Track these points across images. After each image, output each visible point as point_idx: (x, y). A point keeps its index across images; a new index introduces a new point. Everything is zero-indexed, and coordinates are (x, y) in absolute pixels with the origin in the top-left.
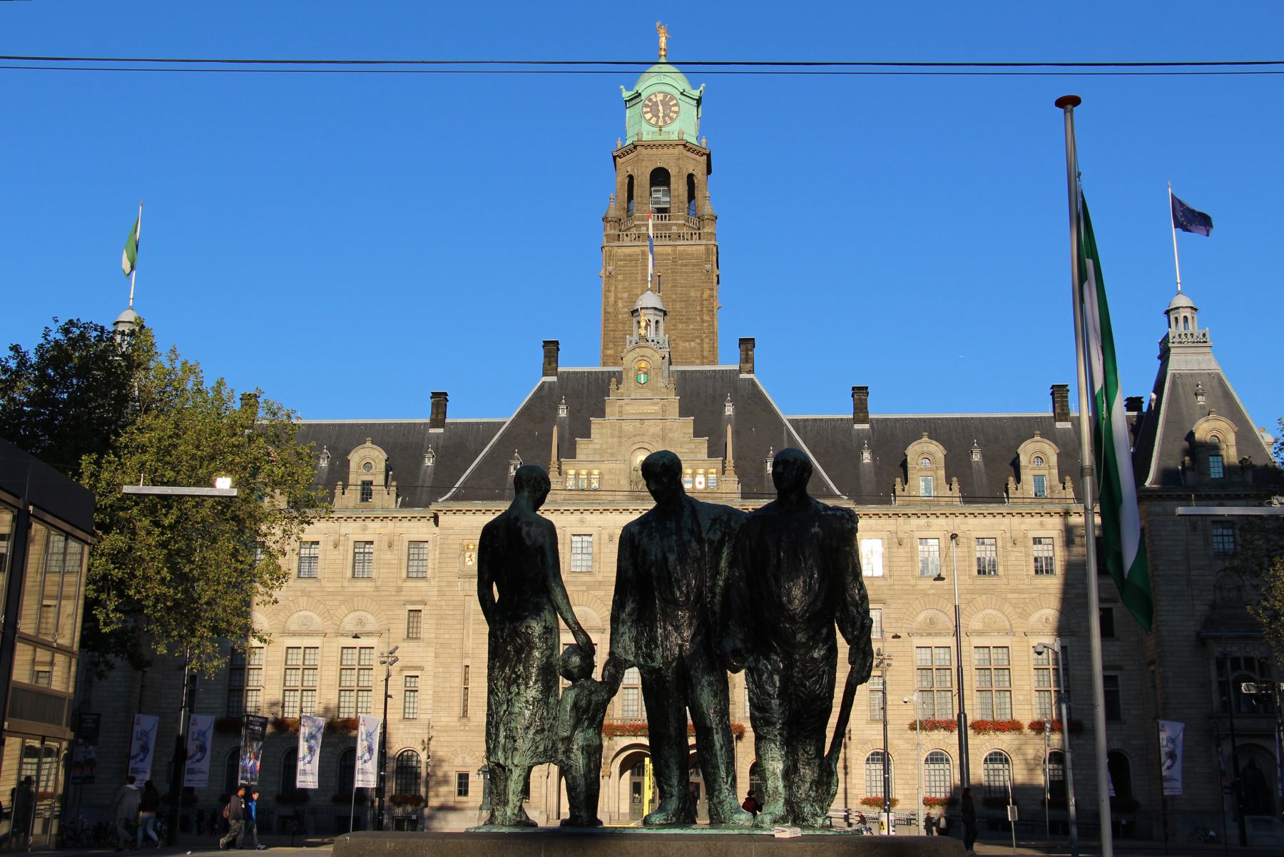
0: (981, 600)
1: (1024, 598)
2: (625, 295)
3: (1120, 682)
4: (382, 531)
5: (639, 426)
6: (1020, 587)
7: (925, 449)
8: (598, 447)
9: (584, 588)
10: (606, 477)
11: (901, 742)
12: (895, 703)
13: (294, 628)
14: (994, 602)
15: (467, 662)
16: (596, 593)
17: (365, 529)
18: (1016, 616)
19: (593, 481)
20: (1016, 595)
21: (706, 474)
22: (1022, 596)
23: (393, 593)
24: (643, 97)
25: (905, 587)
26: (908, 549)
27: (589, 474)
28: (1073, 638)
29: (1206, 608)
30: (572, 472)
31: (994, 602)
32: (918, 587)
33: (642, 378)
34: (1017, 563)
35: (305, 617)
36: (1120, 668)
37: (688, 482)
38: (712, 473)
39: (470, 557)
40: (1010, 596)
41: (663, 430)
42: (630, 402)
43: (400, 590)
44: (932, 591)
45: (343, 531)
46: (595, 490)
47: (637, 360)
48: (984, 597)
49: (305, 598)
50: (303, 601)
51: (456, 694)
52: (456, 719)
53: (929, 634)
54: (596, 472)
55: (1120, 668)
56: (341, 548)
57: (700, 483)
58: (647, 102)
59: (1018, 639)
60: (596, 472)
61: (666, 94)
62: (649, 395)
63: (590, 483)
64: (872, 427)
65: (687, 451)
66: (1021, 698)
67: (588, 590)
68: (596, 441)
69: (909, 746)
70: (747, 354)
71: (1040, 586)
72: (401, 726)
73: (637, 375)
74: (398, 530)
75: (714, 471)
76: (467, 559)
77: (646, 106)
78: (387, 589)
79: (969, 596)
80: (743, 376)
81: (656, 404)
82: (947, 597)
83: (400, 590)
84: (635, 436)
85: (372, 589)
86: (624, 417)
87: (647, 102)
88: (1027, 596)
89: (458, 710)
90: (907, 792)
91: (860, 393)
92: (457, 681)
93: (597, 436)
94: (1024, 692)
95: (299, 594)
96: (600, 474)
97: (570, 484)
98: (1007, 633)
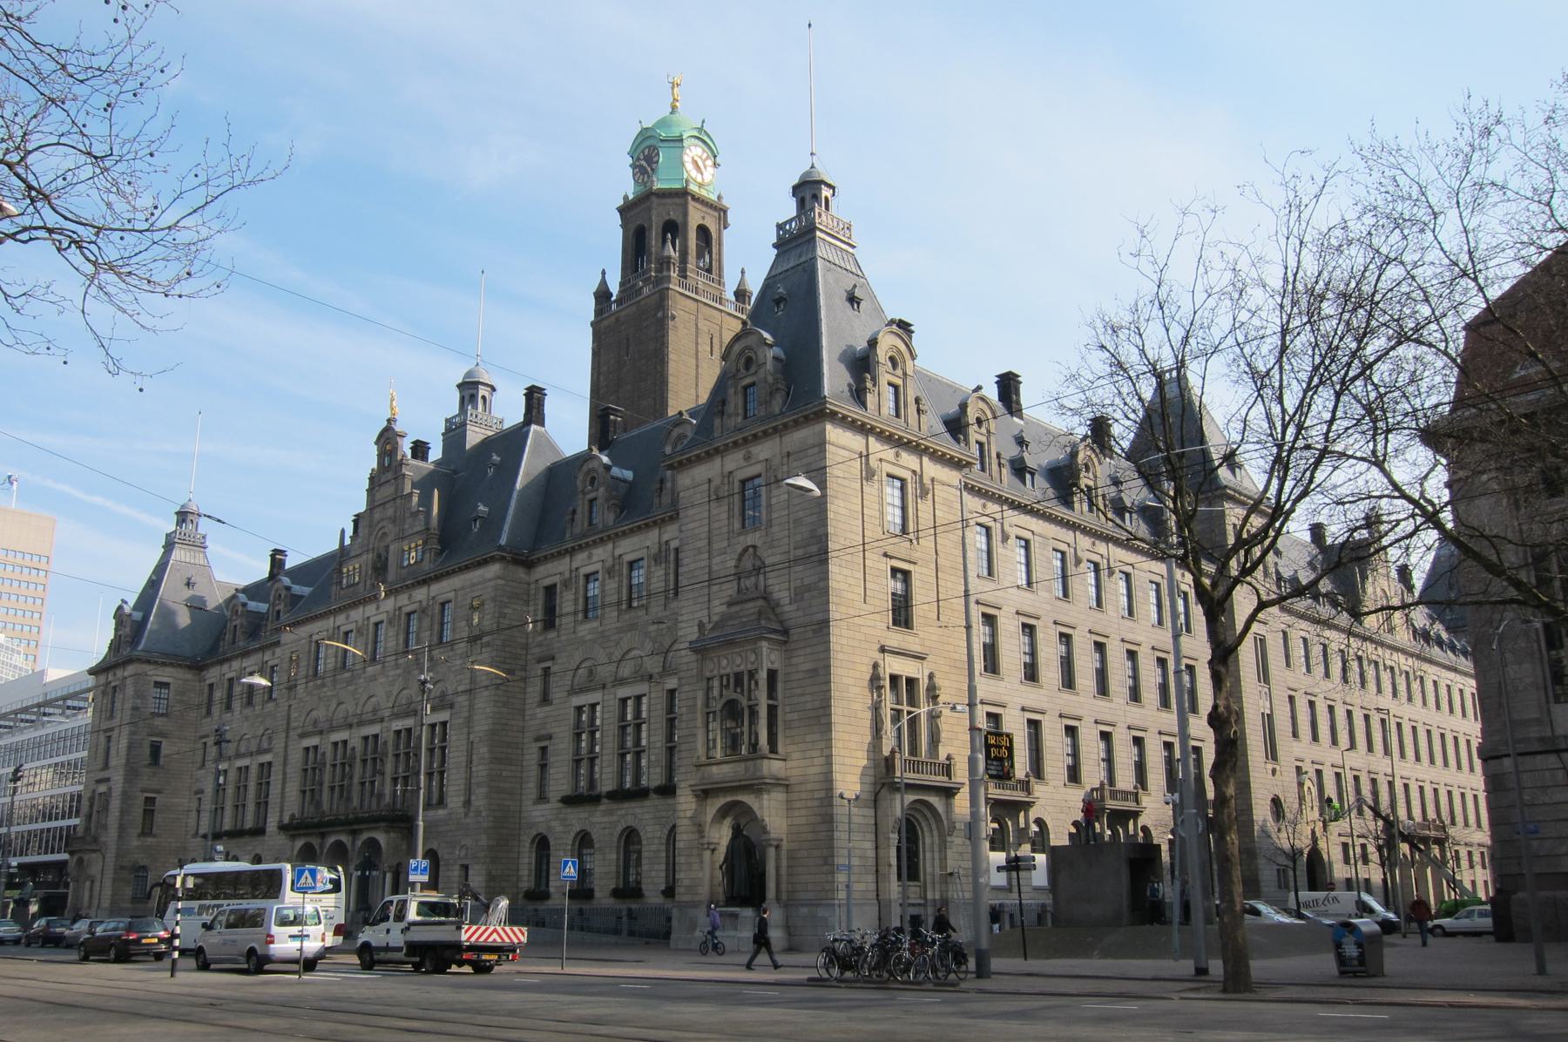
20: (655, 627)
44: (589, 637)
79: (617, 637)
94: (656, 751)
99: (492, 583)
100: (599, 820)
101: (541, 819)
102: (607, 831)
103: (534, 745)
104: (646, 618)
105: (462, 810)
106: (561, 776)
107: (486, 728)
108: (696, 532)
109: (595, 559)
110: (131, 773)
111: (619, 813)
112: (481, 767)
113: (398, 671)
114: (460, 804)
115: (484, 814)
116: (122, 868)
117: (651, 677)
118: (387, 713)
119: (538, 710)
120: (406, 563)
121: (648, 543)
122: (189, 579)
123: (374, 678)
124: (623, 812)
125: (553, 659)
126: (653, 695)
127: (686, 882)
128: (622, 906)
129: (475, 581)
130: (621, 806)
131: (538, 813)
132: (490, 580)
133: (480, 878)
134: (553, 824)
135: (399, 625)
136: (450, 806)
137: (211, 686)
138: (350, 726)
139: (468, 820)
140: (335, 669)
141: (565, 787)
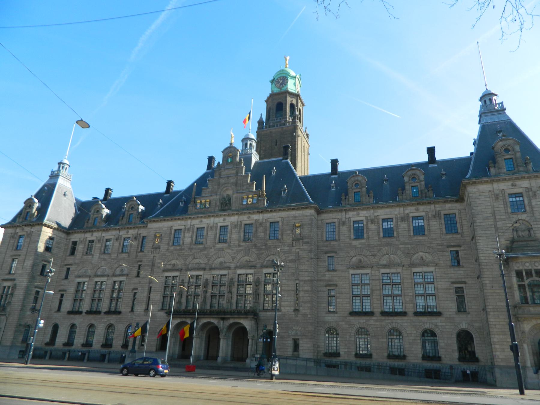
0: (384, 250)
1: (408, 247)
2: (264, 148)
3: (464, 290)
4: (134, 233)
5: (227, 179)
6: (406, 241)
7: (356, 179)
9: (199, 251)
10: (212, 202)
11: (343, 323)
12: (340, 302)
13: (99, 273)
14: (392, 250)
15: (151, 285)
16: (203, 252)
17: (128, 232)
18: (404, 257)
19: (207, 204)
20: (404, 246)
21: (252, 198)
22: (407, 246)
23: (134, 258)
25: (346, 245)
26: (347, 226)
27: (206, 202)
28: (436, 267)
29: (509, 242)
30: (199, 201)
31: (392, 250)
32: (353, 244)
34: (404, 230)
35: (104, 269)
36: (465, 283)
38: (255, 197)
39: (157, 240)
40: (401, 246)
41: (237, 181)
43: (137, 256)
44: (360, 246)
45: (120, 234)
46: (208, 208)
48: (387, 248)
49: (104, 262)
50: (103, 263)
51: (145, 299)
52: (143, 310)
53: (358, 268)
54: (208, 200)
55: (465, 283)
56: (119, 241)
59: (405, 269)
61: (283, 77)
62: (232, 167)
64: (339, 177)
65: (245, 188)
66: (408, 300)
67: (200, 252)
68: (210, 188)
69: (347, 326)
70: (286, 152)
71: (416, 241)
72: (130, 314)
73: (228, 159)
74: (139, 232)
75: (256, 195)
76: (156, 241)
78: (132, 256)
79: (378, 248)
80: (281, 158)
81: (234, 170)
82: (367, 248)
83: (137, 256)
84: (225, 184)
85: (127, 257)
86: (221, 177)
88: (409, 246)
89: (144, 306)
90: (346, 350)
91: (334, 163)
92: (145, 294)
93: (210, 186)
95: (102, 260)
96: (210, 201)
97: (198, 206)
98: (399, 266)
99: (309, 218)
100: (374, 323)
101: (332, 320)
102: (379, 329)
103: (325, 288)
104: (397, 242)
105: (293, 313)
106: (345, 302)
107: (309, 278)
108: (483, 210)
109: (361, 215)
110: (32, 278)
111: (387, 321)
112: (307, 295)
113: (240, 248)
114: (292, 311)
115: (309, 316)
116: (20, 325)
117: (403, 266)
118: (232, 266)
119: (327, 273)
120: (245, 203)
121: (396, 213)
122: (65, 193)
123: (222, 249)
124: (390, 321)
125: (336, 253)
126: (404, 273)
127: (501, 357)
128: (85, 349)
129: (297, 215)
130: (387, 318)
131: (330, 318)
132: (308, 216)
133: (309, 345)
134: (341, 323)
135: (241, 229)
136: (283, 311)
137: (75, 243)
138: (204, 269)
139: (297, 318)
140: (191, 243)
141: (348, 308)
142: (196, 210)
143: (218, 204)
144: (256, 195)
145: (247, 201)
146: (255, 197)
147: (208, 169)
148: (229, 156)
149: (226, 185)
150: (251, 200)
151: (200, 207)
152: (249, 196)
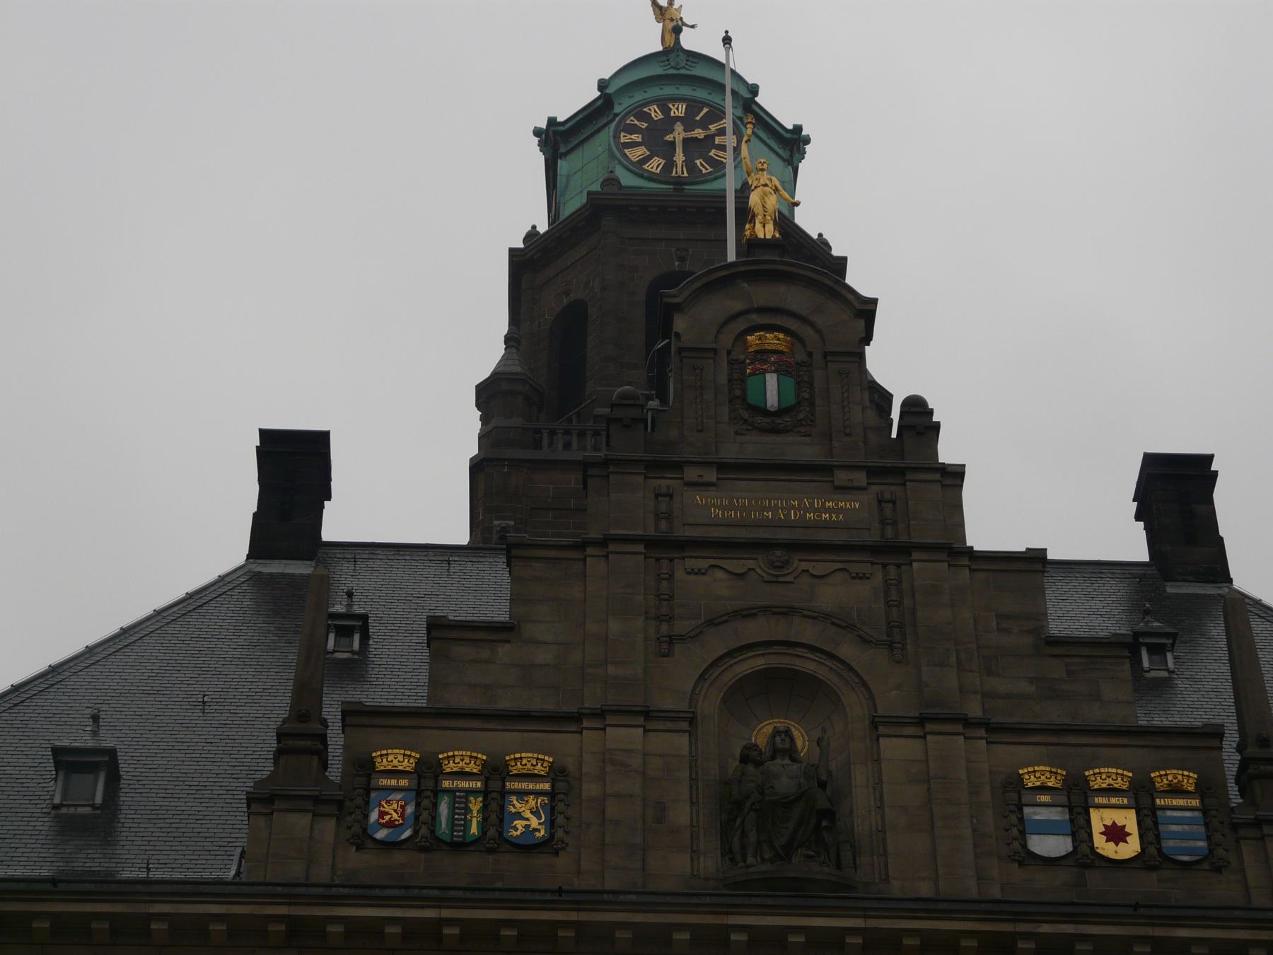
8: (543, 656)
10: (590, 789)
19: (516, 805)
24: (617, 109)
33: (772, 389)
37: (1047, 829)
38: (1176, 791)
42: (711, 476)
46: (527, 847)
47: (741, 325)
57: (1116, 834)
58: (632, 120)
60: (527, 761)
63: (497, 814)
73: (738, 380)
77: (632, 129)
84: (747, 614)
87: (632, 120)
96: (557, 773)
142: (353, 860)
143: (681, 815)
144: (1188, 779)
145: (1079, 829)
146: (1176, 791)
147: (260, 544)
148: (762, 354)
149: (756, 630)
150: (1128, 819)
151: (425, 816)
152: (1101, 778)
